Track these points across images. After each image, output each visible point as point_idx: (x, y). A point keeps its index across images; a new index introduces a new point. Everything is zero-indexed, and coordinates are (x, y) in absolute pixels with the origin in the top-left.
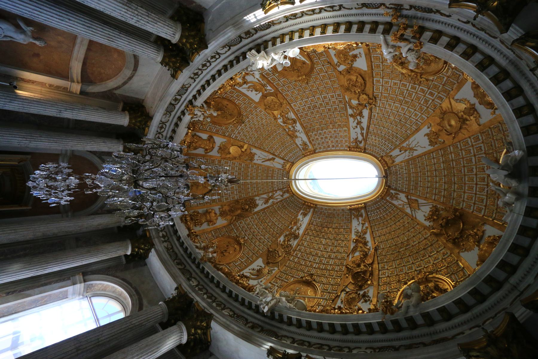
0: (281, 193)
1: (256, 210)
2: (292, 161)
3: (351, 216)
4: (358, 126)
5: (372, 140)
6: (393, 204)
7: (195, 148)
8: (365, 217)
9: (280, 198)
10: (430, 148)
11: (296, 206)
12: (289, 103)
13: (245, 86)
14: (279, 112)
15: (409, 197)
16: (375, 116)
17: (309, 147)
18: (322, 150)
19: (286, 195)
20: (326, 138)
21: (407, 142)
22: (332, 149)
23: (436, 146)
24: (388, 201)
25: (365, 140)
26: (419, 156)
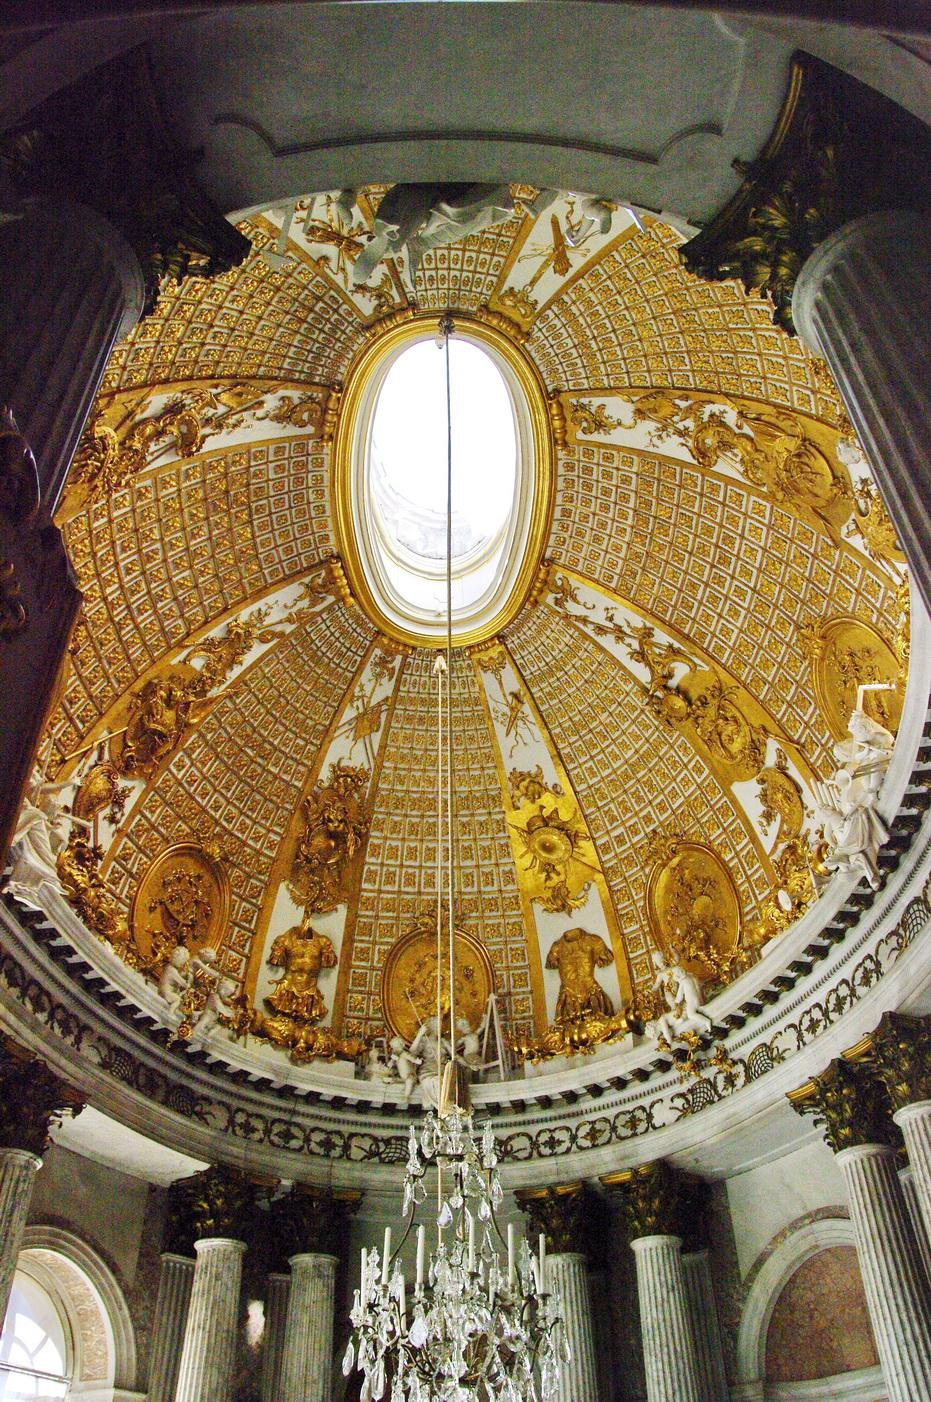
2: (536, 334)
4: (611, 625)
6: (360, 669)
21: (531, 718)
22: (560, 480)
26: (490, 736)
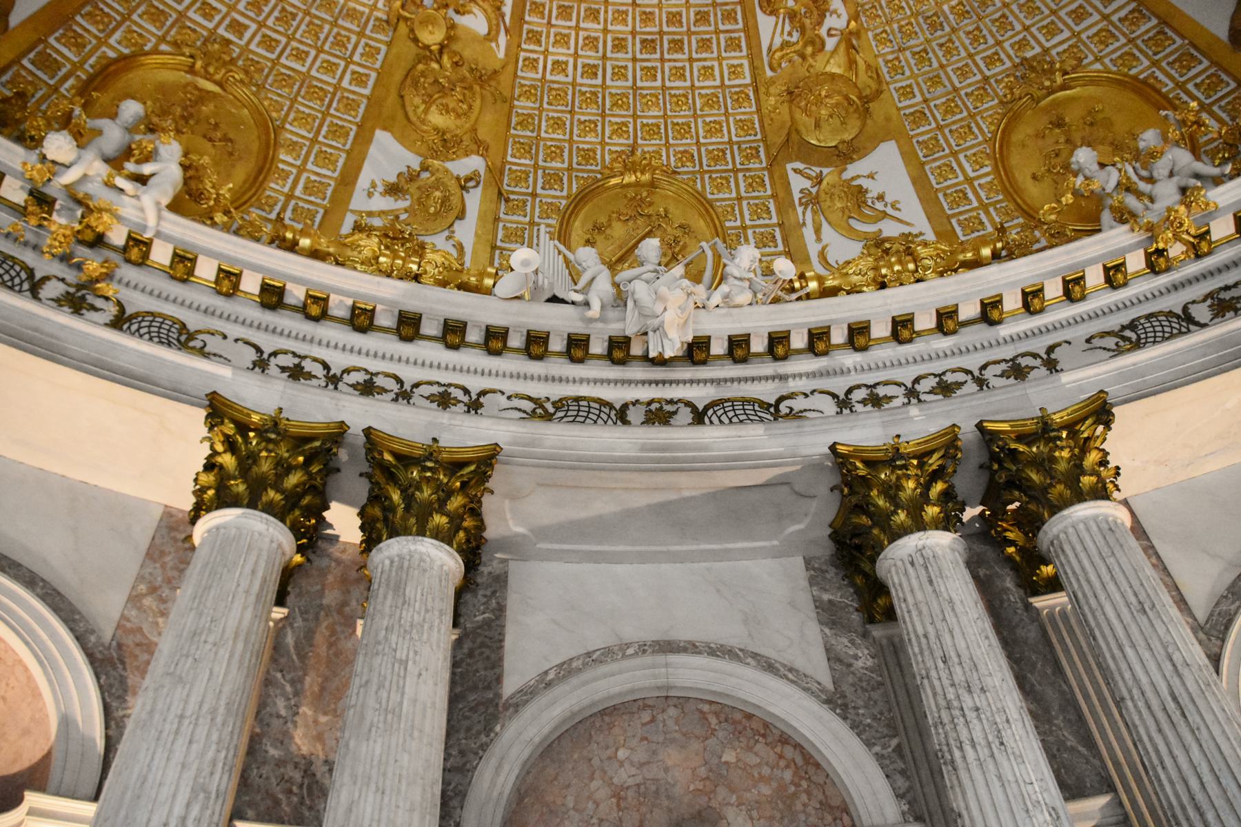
12: (756, 91)
13: (890, 229)
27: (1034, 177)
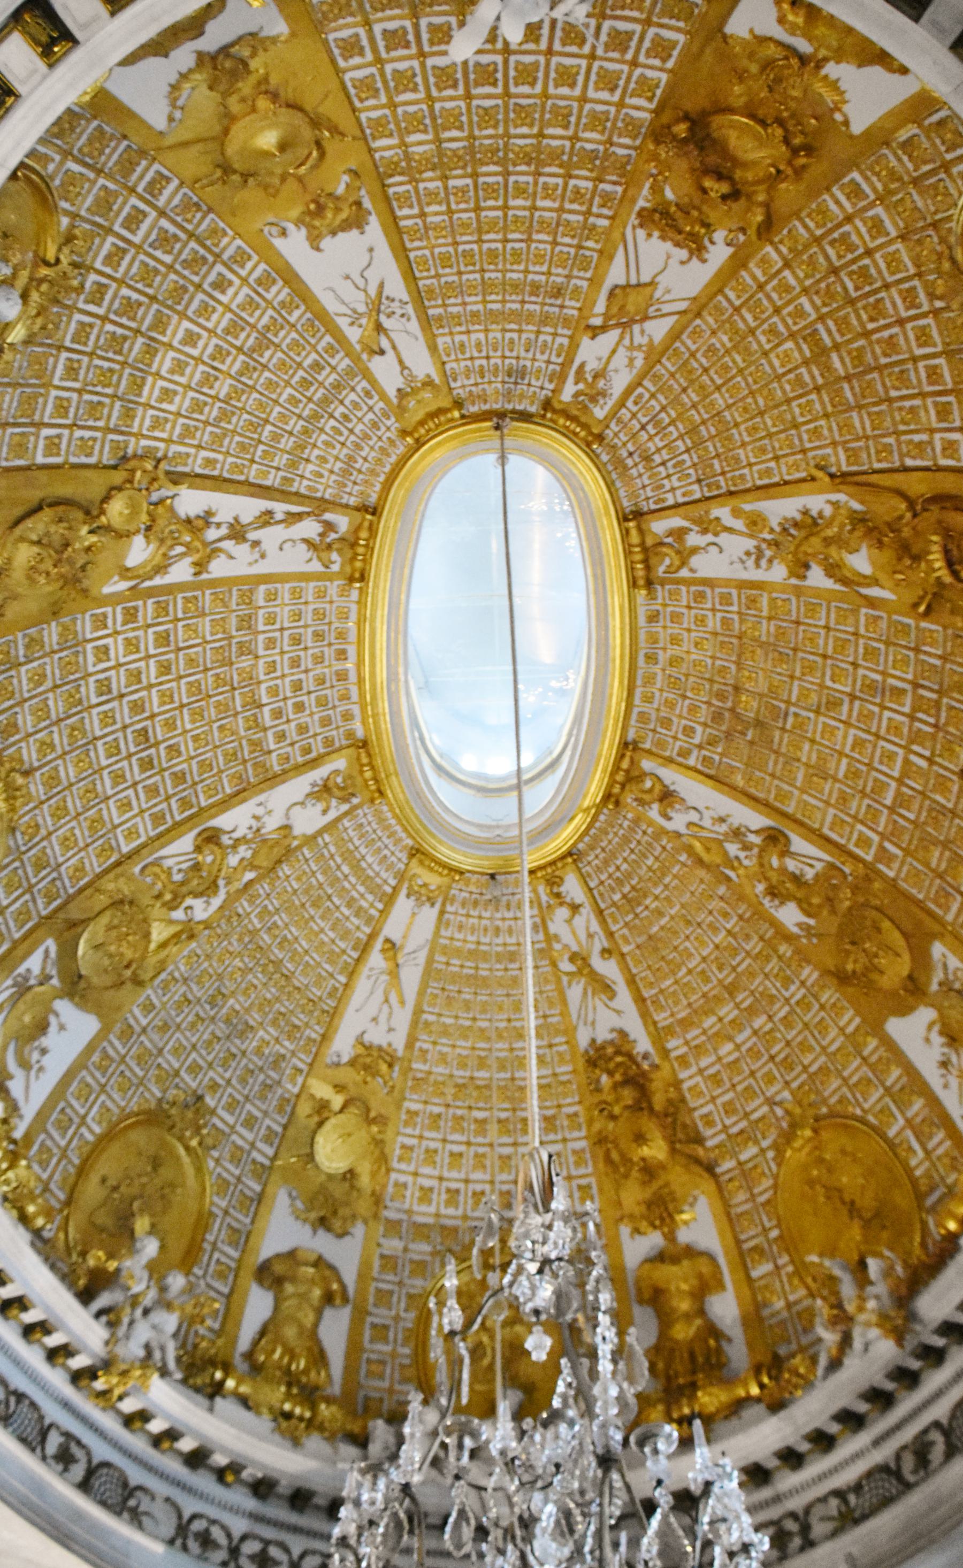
0: (563, 913)
1: (643, 1044)
2: (404, 856)
3: (678, 582)
4: (252, 536)
5: (315, 477)
7: (320, 1357)
8: (686, 518)
9: (586, 920)
10: (374, 226)
11: (626, 840)
12: (118, 864)
14: (157, 911)
15: (597, 321)
16: (209, 462)
17: (337, 772)
18: (356, 710)
19: (572, 887)
20: (297, 686)
21: (343, 322)
23: (367, 204)
24: (613, 414)
25: (321, 505)
27: (104, 1180)
